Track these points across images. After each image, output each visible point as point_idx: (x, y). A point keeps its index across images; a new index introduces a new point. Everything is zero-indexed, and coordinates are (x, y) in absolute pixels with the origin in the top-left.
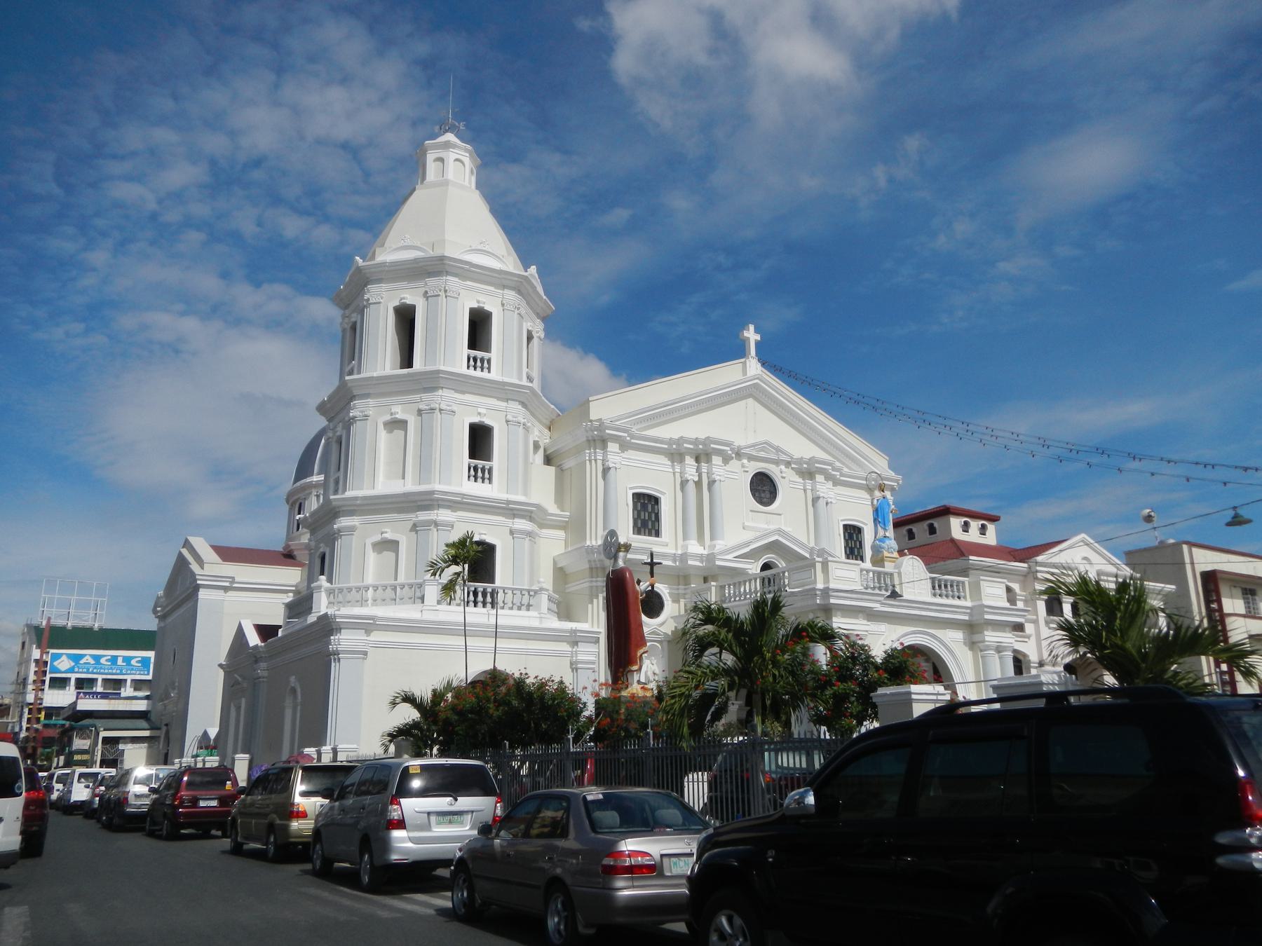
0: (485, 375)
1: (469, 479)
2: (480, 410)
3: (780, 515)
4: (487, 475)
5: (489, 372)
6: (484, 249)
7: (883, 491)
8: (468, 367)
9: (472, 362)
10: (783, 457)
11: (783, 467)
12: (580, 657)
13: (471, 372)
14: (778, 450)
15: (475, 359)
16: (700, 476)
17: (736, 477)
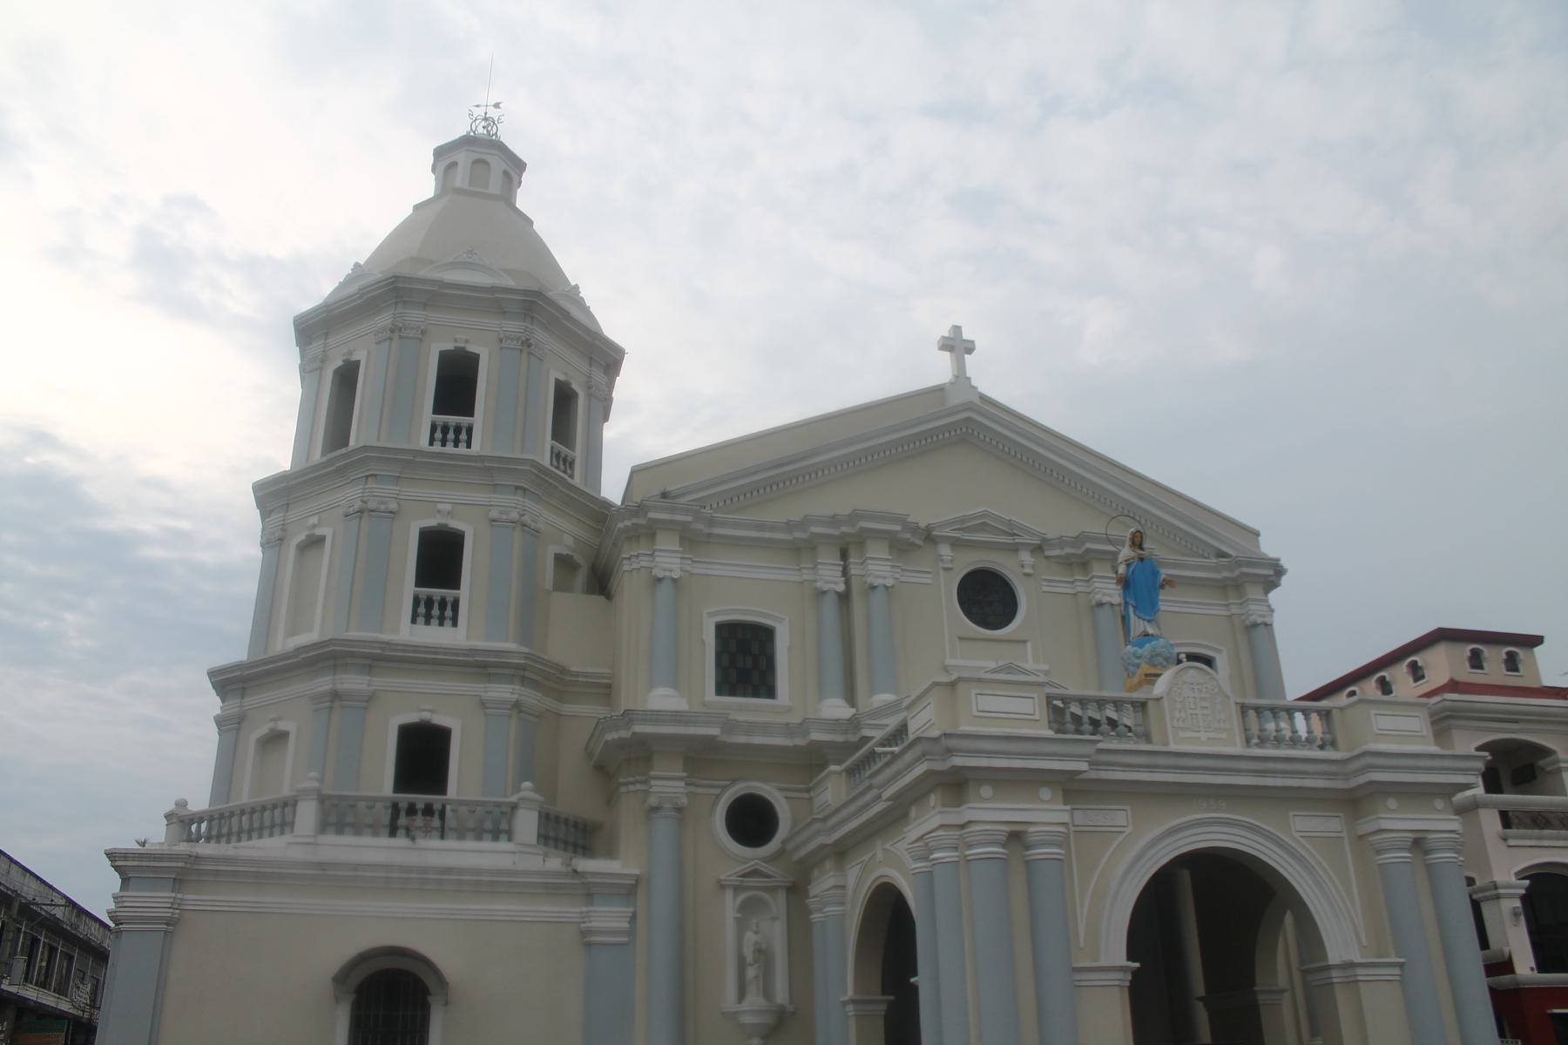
0: (462, 449)
1: (414, 621)
2: (440, 506)
3: (1025, 642)
4: (449, 613)
5: (469, 446)
6: (469, 260)
7: (1141, 547)
8: (431, 444)
9: (438, 435)
10: (1026, 539)
11: (1026, 557)
12: (596, 924)
13: (437, 448)
14: (1011, 529)
15: (445, 429)
16: (847, 583)
17: (929, 581)
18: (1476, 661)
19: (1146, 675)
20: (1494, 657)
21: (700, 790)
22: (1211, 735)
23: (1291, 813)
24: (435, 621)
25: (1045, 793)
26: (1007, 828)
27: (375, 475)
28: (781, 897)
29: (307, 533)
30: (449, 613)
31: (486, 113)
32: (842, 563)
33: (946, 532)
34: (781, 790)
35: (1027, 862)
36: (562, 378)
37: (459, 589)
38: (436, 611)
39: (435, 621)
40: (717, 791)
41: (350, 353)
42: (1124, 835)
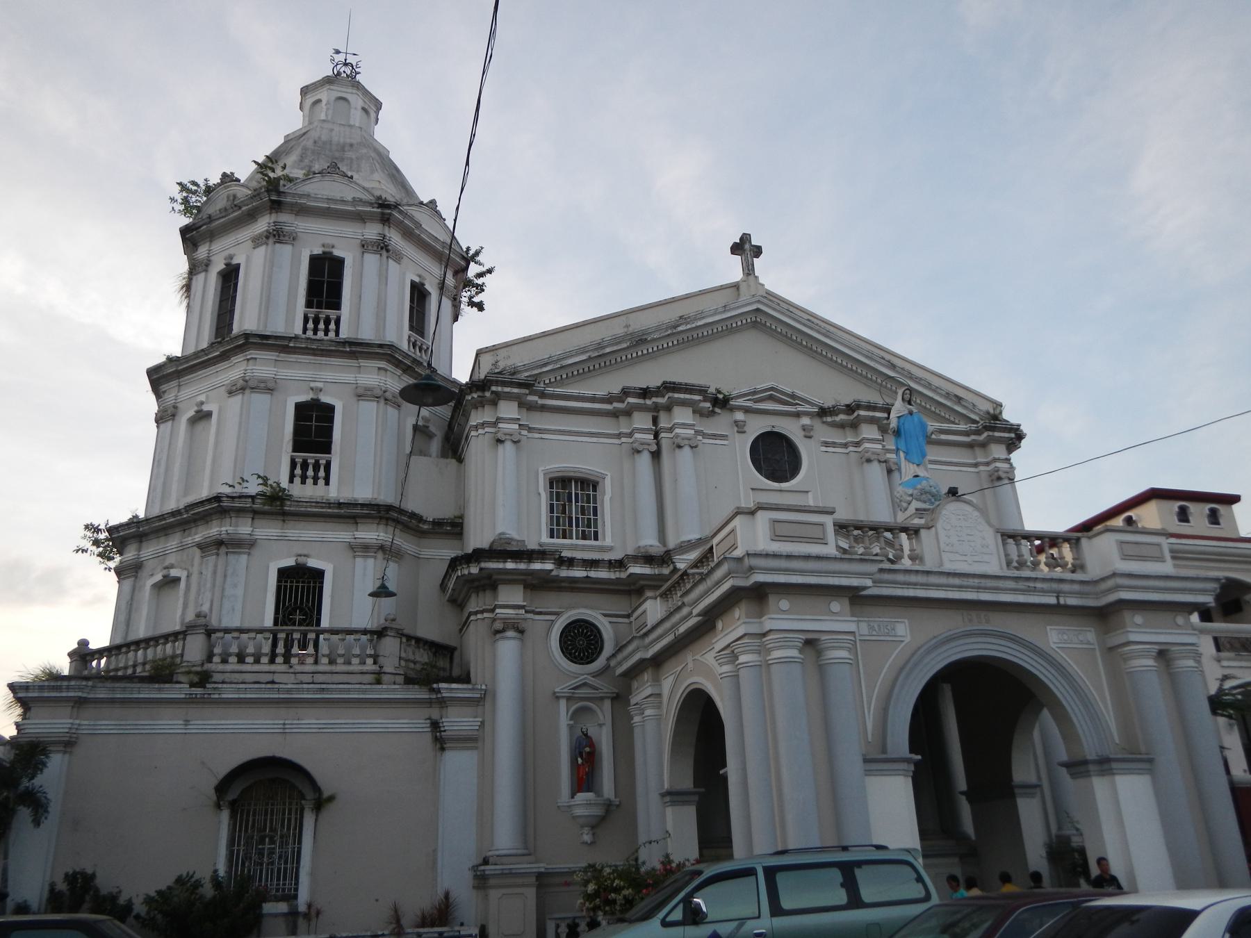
3: (807, 492)
4: (322, 473)
10: (808, 408)
16: (658, 444)
18: (1183, 515)
19: (917, 510)
20: (1198, 512)
21: (537, 617)
22: (976, 559)
23: (1048, 628)
24: (310, 481)
25: (835, 606)
26: (803, 636)
27: (256, 359)
28: (607, 704)
29: (196, 408)
30: (322, 473)
31: (346, 60)
32: (654, 428)
33: (740, 402)
34: (605, 615)
35: (820, 665)
36: (417, 280)
37: (330, 453)
38: (310, 473)
39: (310, 481)
40: (553, 617)
41: (231, 257)
42: (903, 644)
